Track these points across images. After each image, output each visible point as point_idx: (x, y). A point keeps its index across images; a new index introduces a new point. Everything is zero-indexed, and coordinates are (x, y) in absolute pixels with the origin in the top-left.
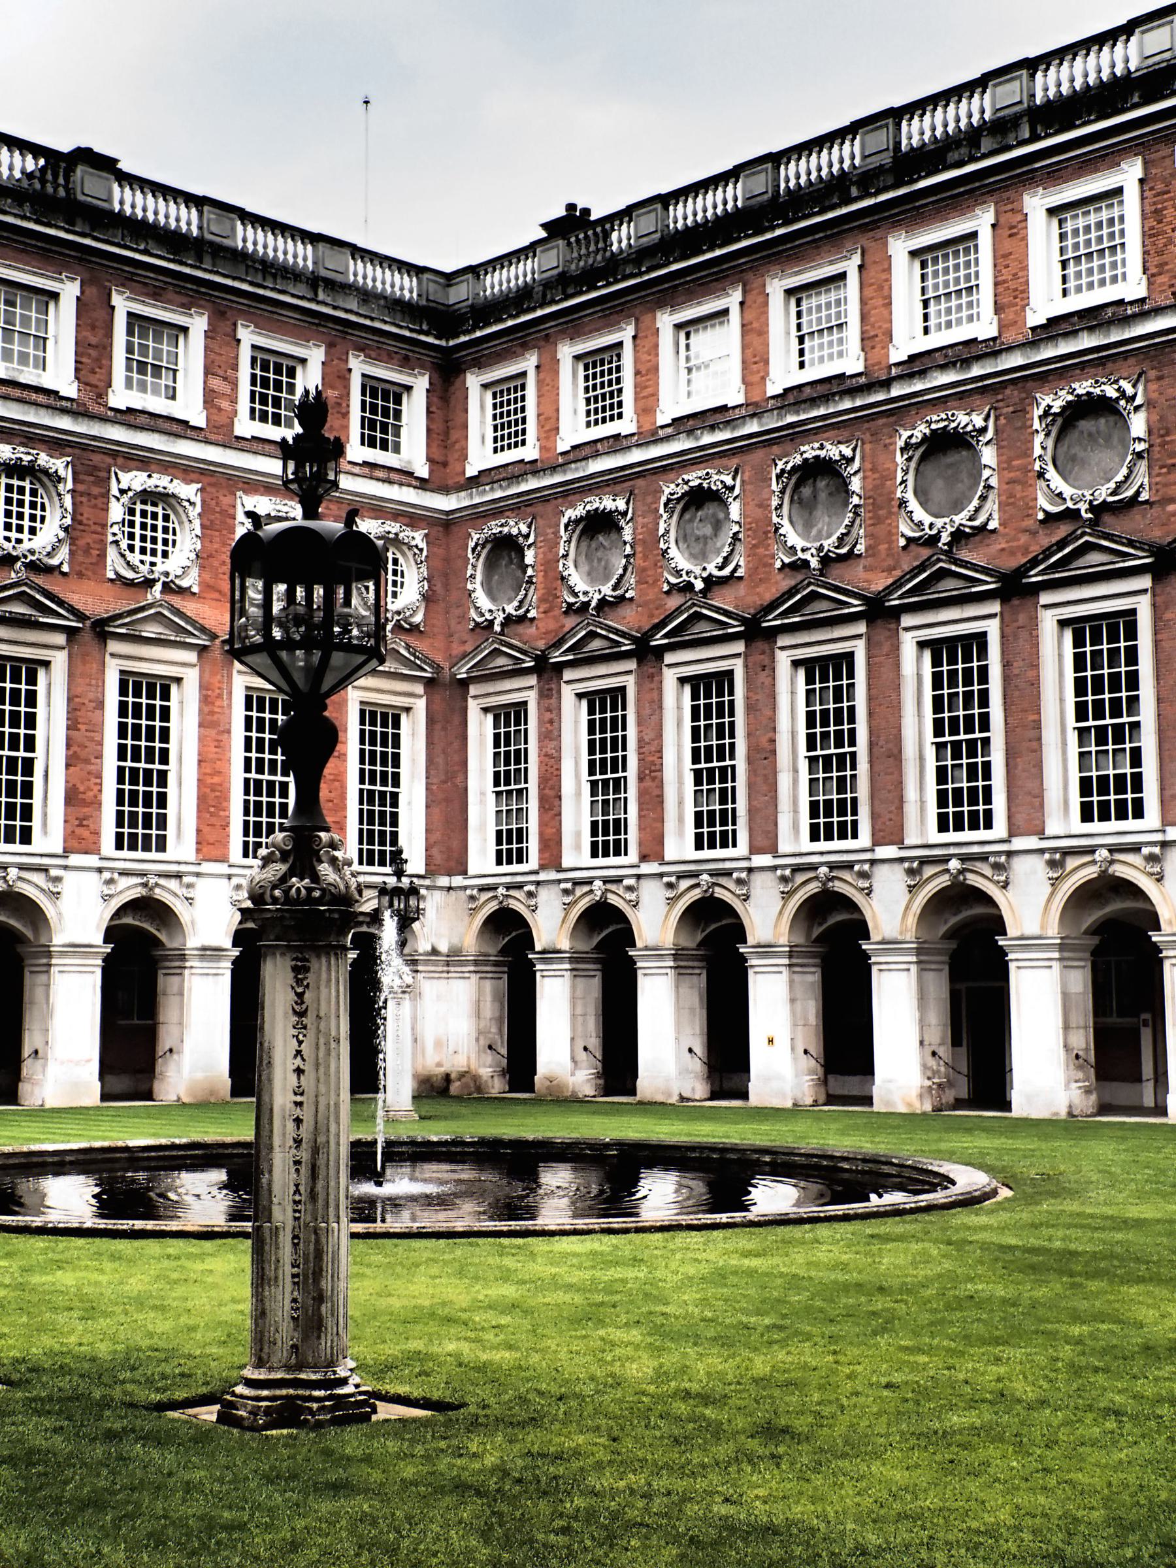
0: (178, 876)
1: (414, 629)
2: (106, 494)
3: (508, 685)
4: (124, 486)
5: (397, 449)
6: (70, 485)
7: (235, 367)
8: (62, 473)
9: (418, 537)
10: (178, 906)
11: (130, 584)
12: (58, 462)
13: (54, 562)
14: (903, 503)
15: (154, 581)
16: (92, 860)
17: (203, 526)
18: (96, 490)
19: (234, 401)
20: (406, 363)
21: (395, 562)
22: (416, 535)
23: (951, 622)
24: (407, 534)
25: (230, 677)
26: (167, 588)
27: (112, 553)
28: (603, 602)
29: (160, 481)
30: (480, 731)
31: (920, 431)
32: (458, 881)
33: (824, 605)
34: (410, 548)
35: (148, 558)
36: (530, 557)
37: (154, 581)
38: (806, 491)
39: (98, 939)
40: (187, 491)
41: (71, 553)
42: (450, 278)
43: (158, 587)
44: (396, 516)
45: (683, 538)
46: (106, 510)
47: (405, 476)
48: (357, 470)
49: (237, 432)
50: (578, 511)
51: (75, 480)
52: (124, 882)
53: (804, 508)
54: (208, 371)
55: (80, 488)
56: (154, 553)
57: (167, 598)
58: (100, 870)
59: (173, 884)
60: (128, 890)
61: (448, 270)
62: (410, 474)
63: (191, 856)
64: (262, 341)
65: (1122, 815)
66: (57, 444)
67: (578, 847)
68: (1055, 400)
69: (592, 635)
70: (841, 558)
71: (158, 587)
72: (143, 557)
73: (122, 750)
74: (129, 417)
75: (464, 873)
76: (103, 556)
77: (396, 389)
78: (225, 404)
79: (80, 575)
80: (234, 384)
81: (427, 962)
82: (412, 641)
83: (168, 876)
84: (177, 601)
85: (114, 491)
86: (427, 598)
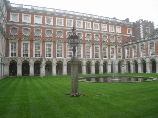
3: (14, 41)
14: (46, 34)
23: (60, 44)
28: (27, 36)
30: (10, 44)
31: (58, 30)
33: (49, 40)
36: (18, 30)
38: (48, 32)
45: (36, 33)
50: (25, 28)
53: (48, 33)
62: (41, 24)
65: (80, 57)
68: (68, 32)
69: (26, 38)
70: (51, 37)
75: (8, 57)
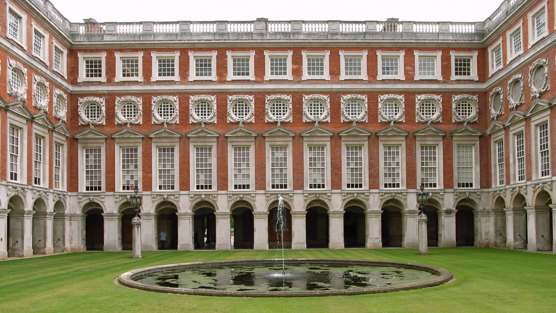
0: (402, 193)
1: (474, 123)
2: (377, 102)
4: (382, 99)
5: (469, 74)
6: (367, 101)
7: (414, 63)
8: (364, 99)
9: (475, 97)
10: (402, 201)
11: (385, 123)
12: (363, 96)
13: (364, 120)
15: (391, 121)
16: (377, 191)
17: (405, 105)
18: (374, 101)
19: (414, 71)
20: (470, 50)
21: (469, 105)
22: (474, 97)
24: (471, 97)
25: (415, 142)
26: (395, 122)
27: (379, 117)
29: (392, 96)
32: (490, 190)
34: (472, 100)
37: (391, 121)
39: (380, 210)
40: (401, 97)
41: (368, 118)
42: (484, 23)
43: (392, 122)
44: (467, 93)
46: (377, 105)
47: (471, 81)
48: (454, 82)
49: (415, 79)
51: (368, 100)
52: (386, 196)
54: (405, 65)
55: (370, 101)
57: (395, 125)
58: (379, 193)
59: (400, 196)
60: (387, 197)
61: (483, 21)
63: (405, 188)
64: (421, 54)
66: (362, 93)
67: (515, 179)
71: (392, 122)
73: (385, 164)
74: (383, 81)
76: (377, 117)
77: (468, 58)
78: (411, 73)
79: (371, 123)
80: (414, 67)
81: (481, 212)
82: (474, 126)
83: (399, 193)
84: (398, 125)
85: (379, 101)
86: (479, 113)
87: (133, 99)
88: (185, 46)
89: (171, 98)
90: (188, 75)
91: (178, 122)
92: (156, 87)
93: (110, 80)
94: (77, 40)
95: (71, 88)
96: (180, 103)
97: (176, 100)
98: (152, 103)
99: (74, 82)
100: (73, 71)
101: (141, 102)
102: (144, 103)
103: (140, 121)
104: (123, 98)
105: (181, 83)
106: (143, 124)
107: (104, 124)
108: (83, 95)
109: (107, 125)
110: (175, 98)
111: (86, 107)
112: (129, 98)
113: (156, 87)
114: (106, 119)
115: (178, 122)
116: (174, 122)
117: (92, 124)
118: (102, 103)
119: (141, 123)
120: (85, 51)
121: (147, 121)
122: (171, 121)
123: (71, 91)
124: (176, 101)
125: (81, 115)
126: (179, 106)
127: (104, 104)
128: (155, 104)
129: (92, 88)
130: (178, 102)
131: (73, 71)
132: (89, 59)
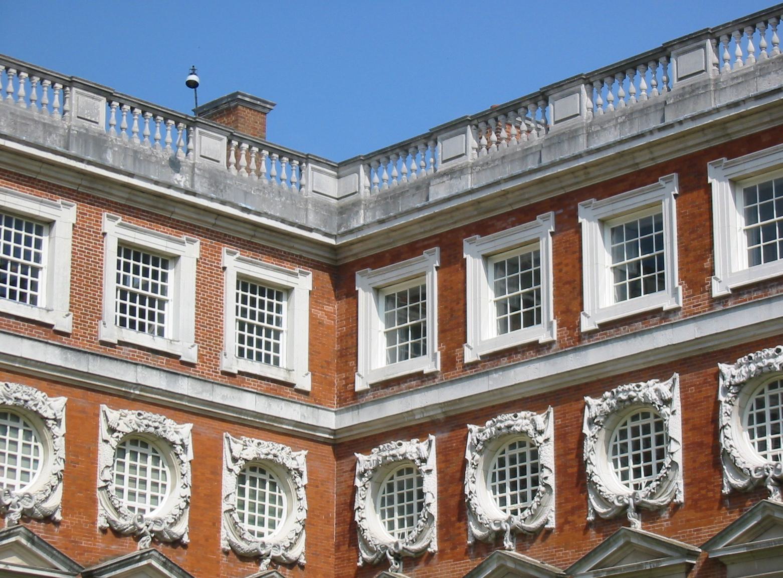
35: (257, 528)
56: (261, 523)
72: (252, 527)
87: (522, 421)
88: (693, 146)
89: (650, 389)
90: (712, 272)
91: (681, 498)
92: (594, 356)
93: (453, 365)
94: (354, 224)
95: (329, 420)
96: (685, 407)
97: (667, 395)
98: (586, 430)
99: (350, 398)
100: (337, 351)
101: (550, 432)
102: (560, 435)
103: (549, 516)
104: (489, 429)
105: (692, 316)
106: (560, 527)
107: (434, 547)
108: (367, 440)
109: (441, 551)
110: (664, 387)
111: (384, 486)
112: (506, 419)
113: (594, 356)
114: (440, 527)
115: (681, 498)
116: (662, 500)
117: (398, 557)
118: (424, 461)
119: (552, 524)
120: (378, 261)
121: (572, 512)
122: (652, 495)
123: (334, 432)
124: (668, 402)
125: (364, 525)
126: (685, 421)
127: (432, 463)
128: (595, 429)
129: (395, 407)
130: (677, 404)
131: (337, 351)
132: (395, 290)
